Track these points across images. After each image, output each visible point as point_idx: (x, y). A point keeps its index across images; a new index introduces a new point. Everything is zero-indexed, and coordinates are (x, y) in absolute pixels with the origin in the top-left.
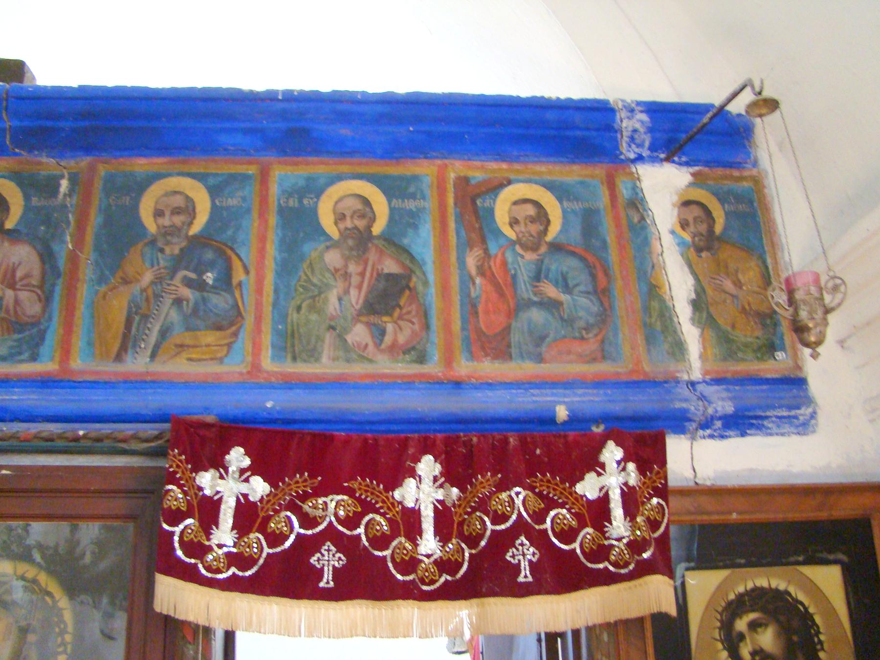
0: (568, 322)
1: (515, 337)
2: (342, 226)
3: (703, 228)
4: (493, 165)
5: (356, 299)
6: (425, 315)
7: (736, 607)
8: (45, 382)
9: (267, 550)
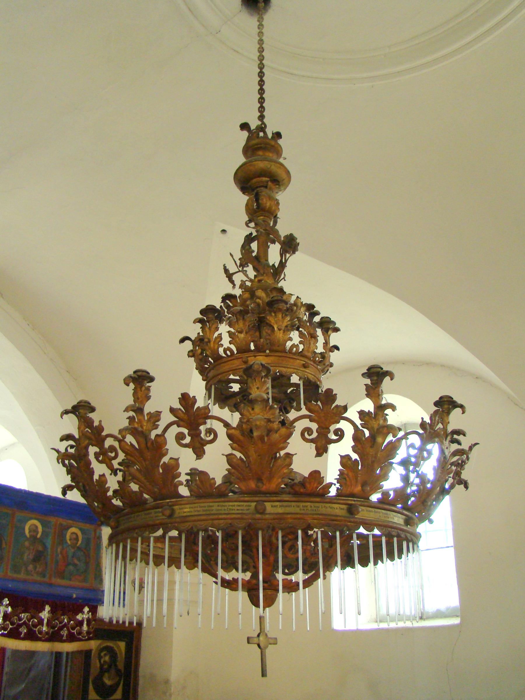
2: (30, 534)
5: (31, 557)
6: (46, 563)
7: (102, 650)
9: (10, 626)
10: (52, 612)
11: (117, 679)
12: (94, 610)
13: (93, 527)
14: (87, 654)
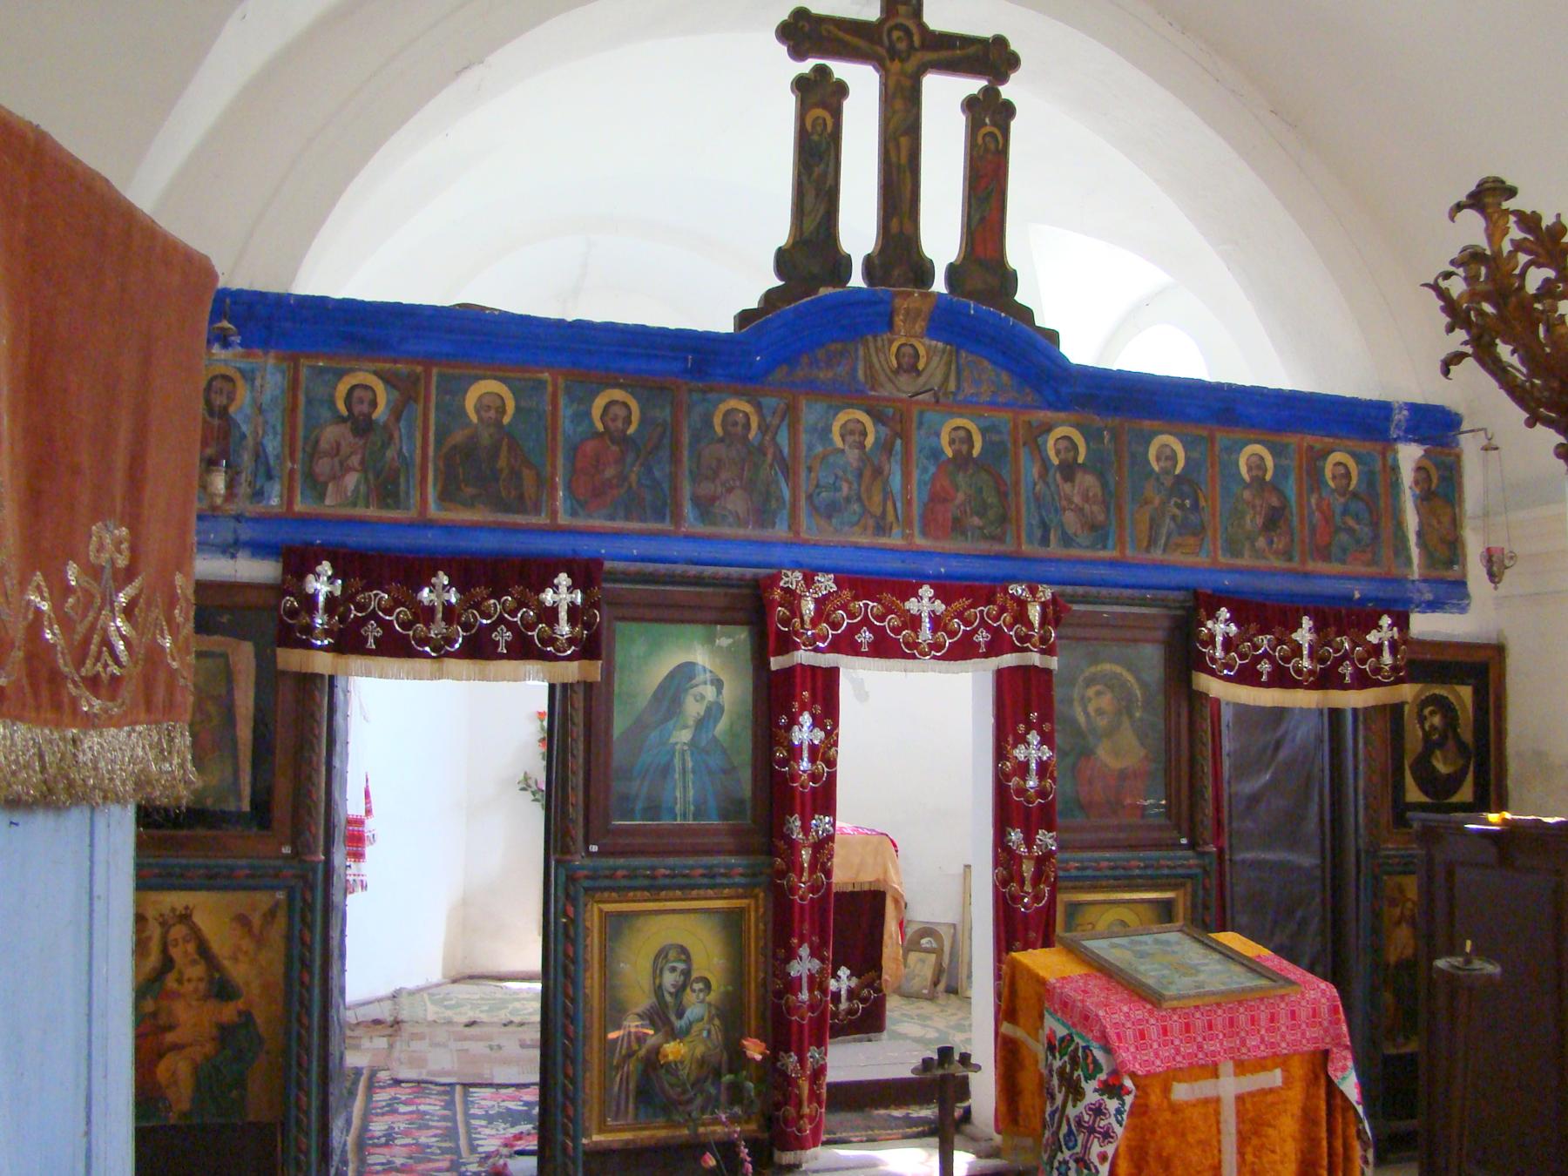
0: (1358, 542)
1: (1334, 550)
3: (1426, 486)
4: (1327, 440)
5: (1259, 521)
8: (1112, 563)
10: (1317, 629)
11: (1461, 762)
12: (1401, 622)
13: (1379, 447)
14: (1396, 710)
